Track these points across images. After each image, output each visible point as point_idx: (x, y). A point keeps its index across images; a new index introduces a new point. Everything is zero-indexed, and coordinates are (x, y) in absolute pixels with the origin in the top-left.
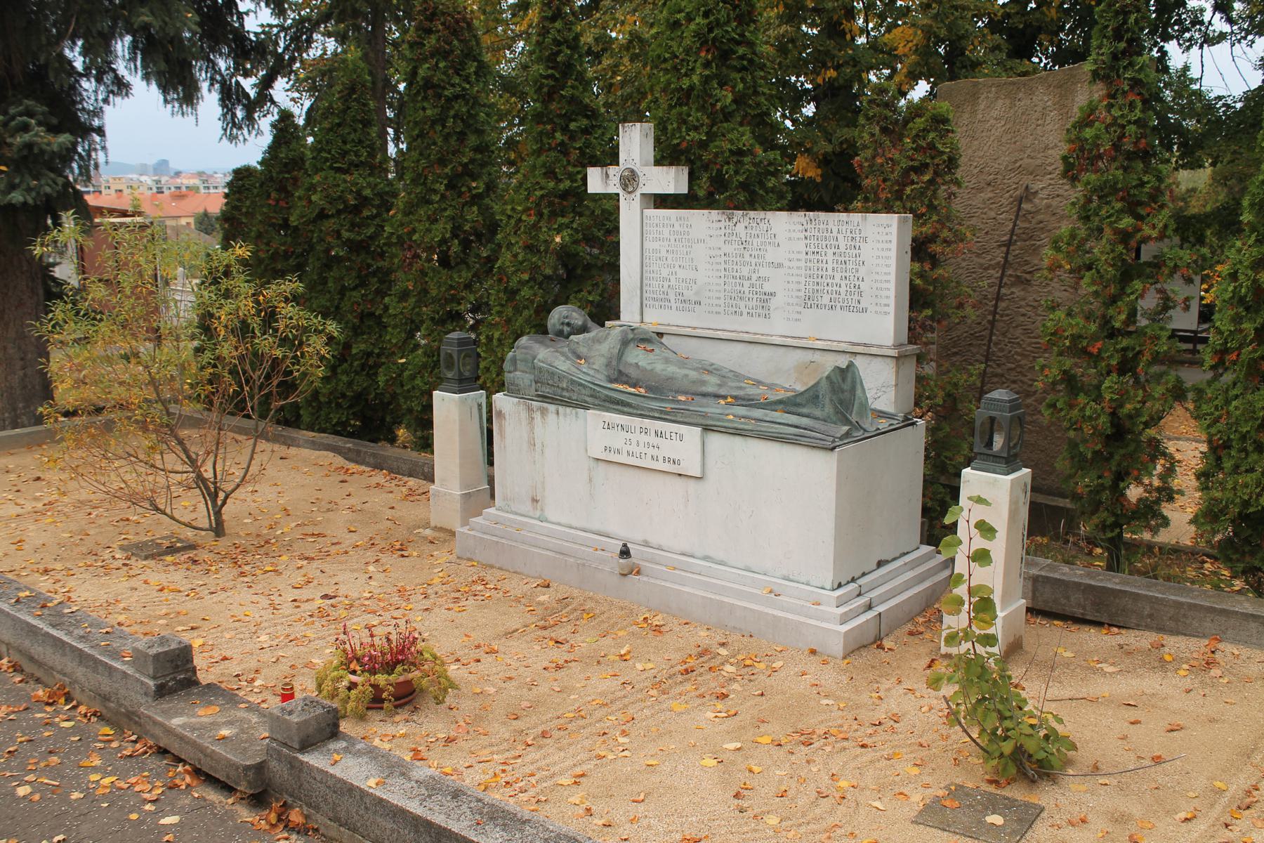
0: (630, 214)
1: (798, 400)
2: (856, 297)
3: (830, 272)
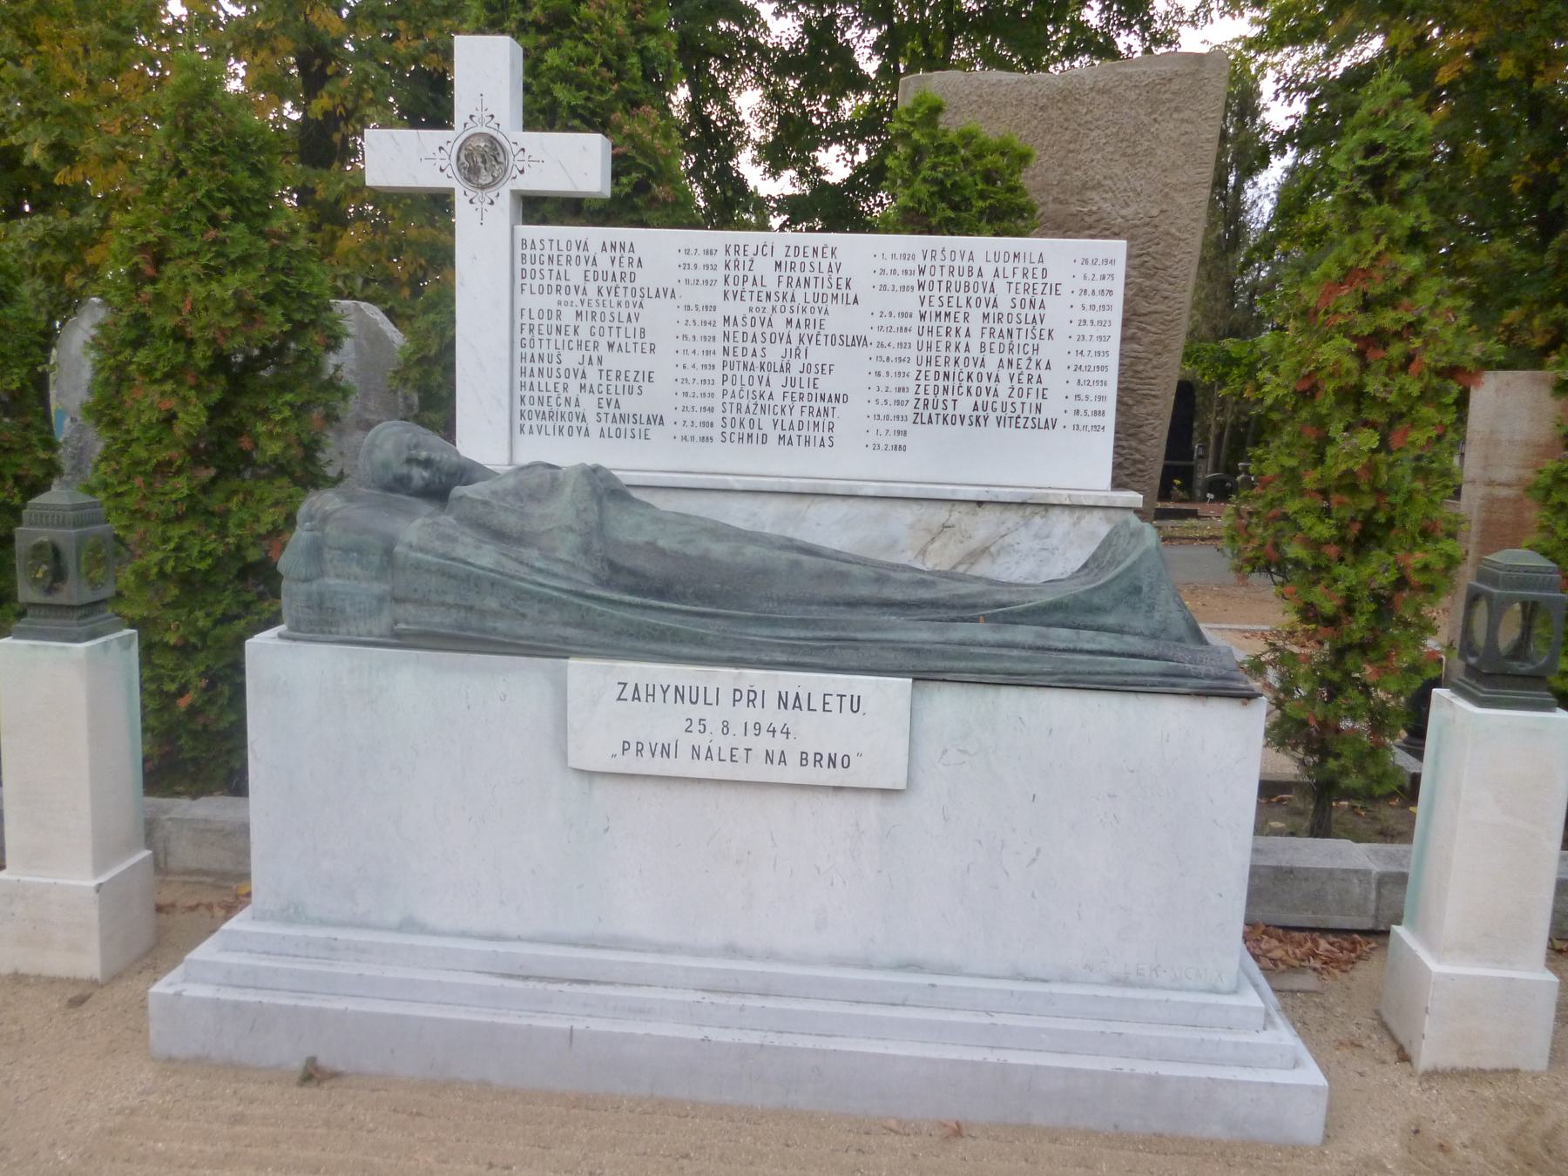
0: (482, 236)
1: (1096, 600)
2: (1033, 399)
3: (975, 352)
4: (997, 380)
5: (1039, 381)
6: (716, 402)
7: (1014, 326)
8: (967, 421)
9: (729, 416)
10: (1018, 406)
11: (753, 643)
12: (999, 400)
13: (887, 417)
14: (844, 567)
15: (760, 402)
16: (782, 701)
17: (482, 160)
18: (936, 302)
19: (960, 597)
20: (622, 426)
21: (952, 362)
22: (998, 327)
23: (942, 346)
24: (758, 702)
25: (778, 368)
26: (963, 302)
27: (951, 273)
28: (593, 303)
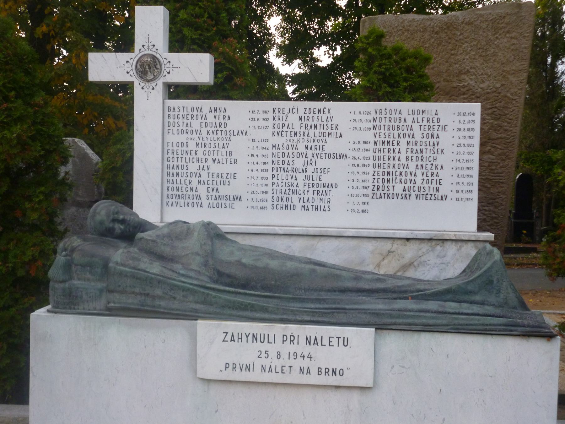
0: (148, 106)
1: (470, 288)
2: (434, 185)
3: (403, 161)
4: (415, 175)
5: (437, 176)
6: (269, 189)
7: (423, 147)
8: (400, 197)
9: (275, 196)
10: (427, 189)
11: (292, 311)
12: (416, 186)
13: (358, 195)
14: (338, 272)
15: (292, 188)
16: (308, 341)
17: (148, 68)
18: (382, 136)
19: (398, 287)
20: (220, 202)
21: (391, 166)
22: (415, 148)
23: (386, 158)
24: (296, 341)
25: (301, 171)
26: (396, 136)
27: (390, 121)
28: (205, 139)
